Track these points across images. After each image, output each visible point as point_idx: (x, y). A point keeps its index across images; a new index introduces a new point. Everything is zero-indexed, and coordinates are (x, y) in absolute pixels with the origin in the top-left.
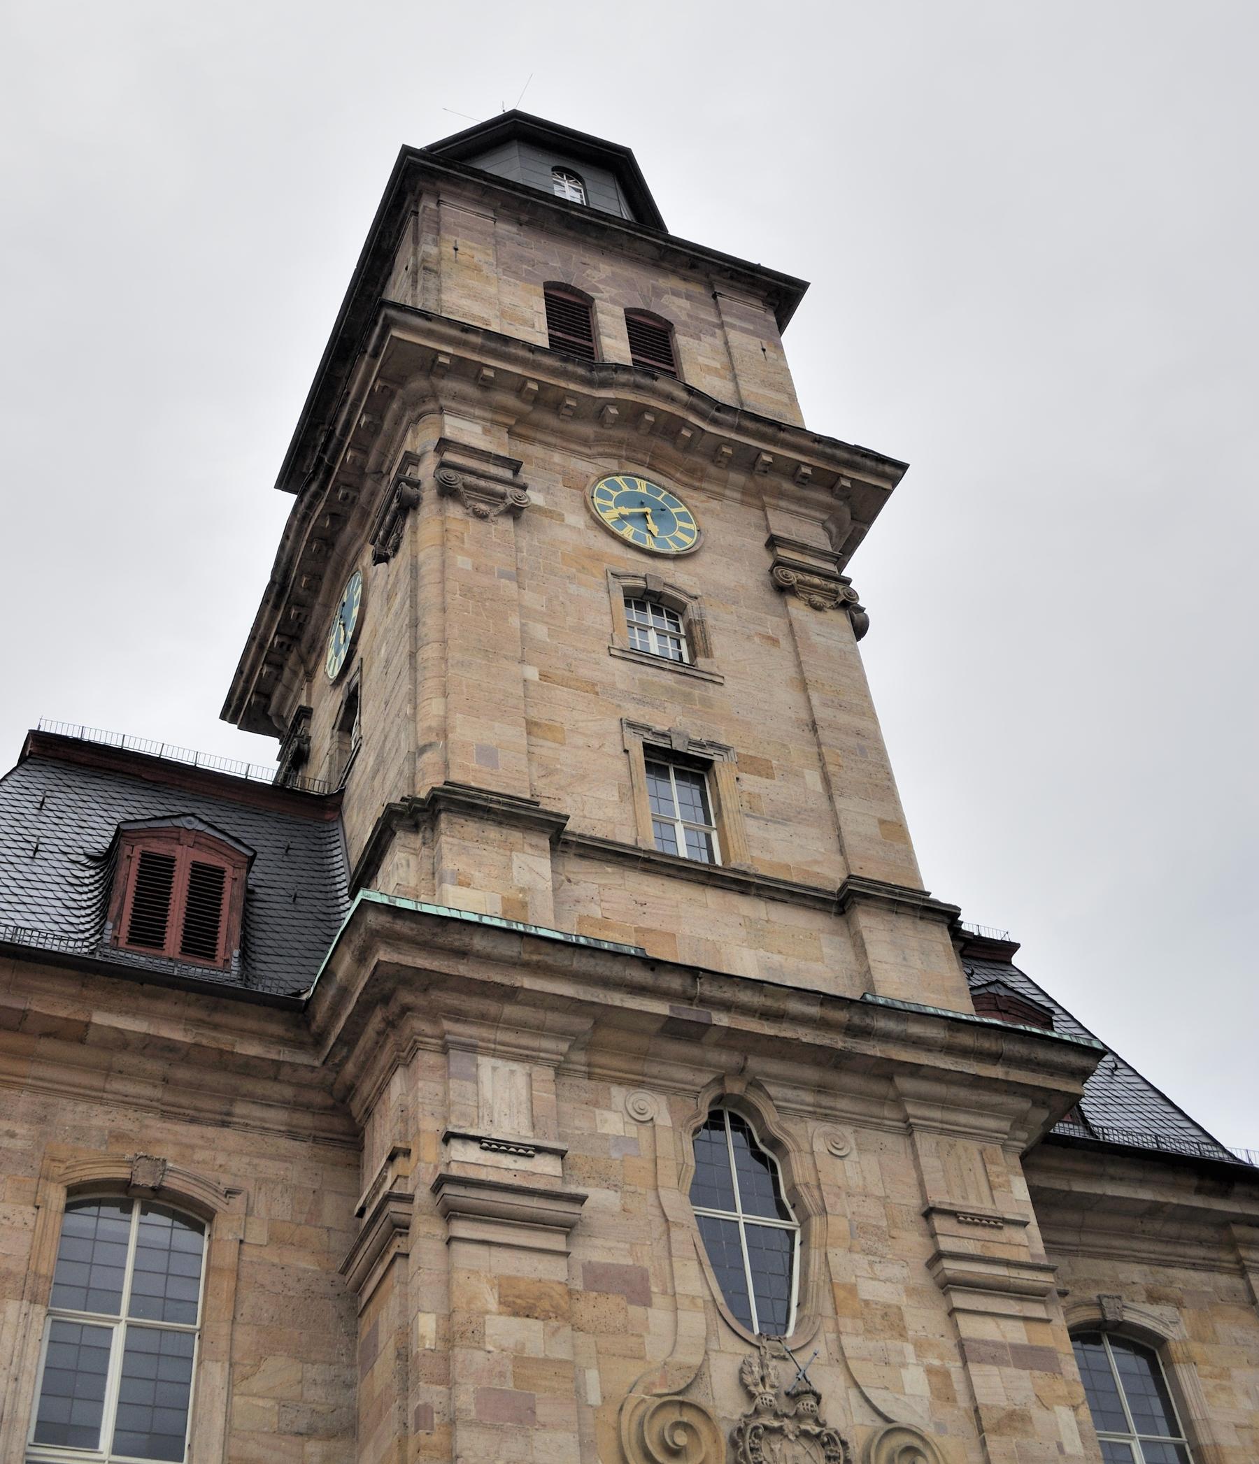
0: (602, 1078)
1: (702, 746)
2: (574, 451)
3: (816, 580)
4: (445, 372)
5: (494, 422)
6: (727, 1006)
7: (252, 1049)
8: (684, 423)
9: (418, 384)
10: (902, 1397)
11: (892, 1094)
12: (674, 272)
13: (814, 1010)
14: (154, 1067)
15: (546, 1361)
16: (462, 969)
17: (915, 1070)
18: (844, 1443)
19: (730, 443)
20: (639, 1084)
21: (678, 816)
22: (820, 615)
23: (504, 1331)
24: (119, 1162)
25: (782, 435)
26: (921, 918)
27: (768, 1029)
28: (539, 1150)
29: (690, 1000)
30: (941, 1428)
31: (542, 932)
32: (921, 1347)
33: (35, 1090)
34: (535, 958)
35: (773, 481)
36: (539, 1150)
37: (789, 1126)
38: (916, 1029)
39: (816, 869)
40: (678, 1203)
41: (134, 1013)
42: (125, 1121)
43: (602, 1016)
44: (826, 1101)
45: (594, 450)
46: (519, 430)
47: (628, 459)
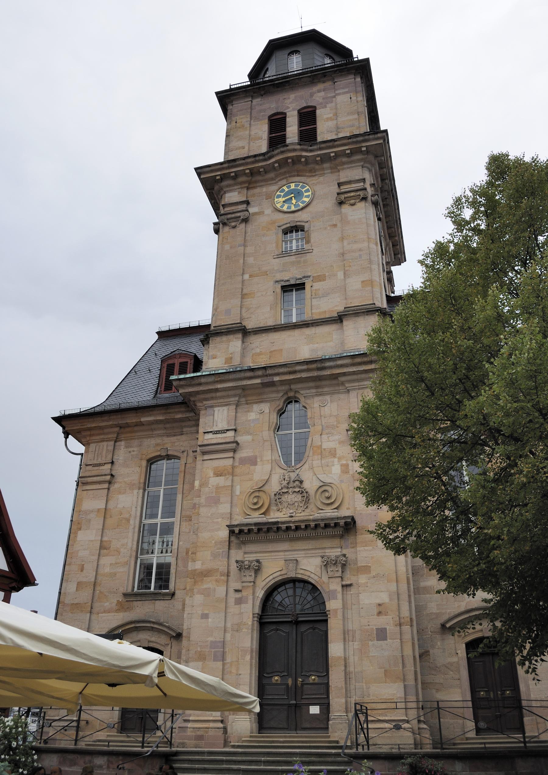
0: (250, 403)
1: (301, 279)
2: (270, 184)
3: (352, 194)
4: (222, 180)
5: (241, 188)
6: (278, 374)
7: (179, 416)
8: (301, 156)
9: (216, 187)
10: (330, 475)
11: (340, 383)
12: (319, 82)
13: (305, 367)
14: (160, 426)
15: (224, 487)
16: (201, 388)
17: (344, 374)
18: (307, 492)
19: (318, 156)
20: (262, 402)
21: (294, 306)
23: (214, 481)
24: (157, 451)
25: (336, 143)
26: (367, 315)
27: (292, 377)
28: (228, 430)
29: (267, 376)
30: (342, 481)
31: (220, 372)
32: (340, 459)
33: (138, 439)
34: (219, 379)
35: (339, 160)
36: (228, 430)
37: (308, 401)
38: (340, 362)
39: (336, 308)
40: (267, 434)
41: (150, 415)
42: (158, 440)
43: (244, 388)
44: (320, 390)
45: (277, 180)
46: (251, 186)
47: (290, 177)
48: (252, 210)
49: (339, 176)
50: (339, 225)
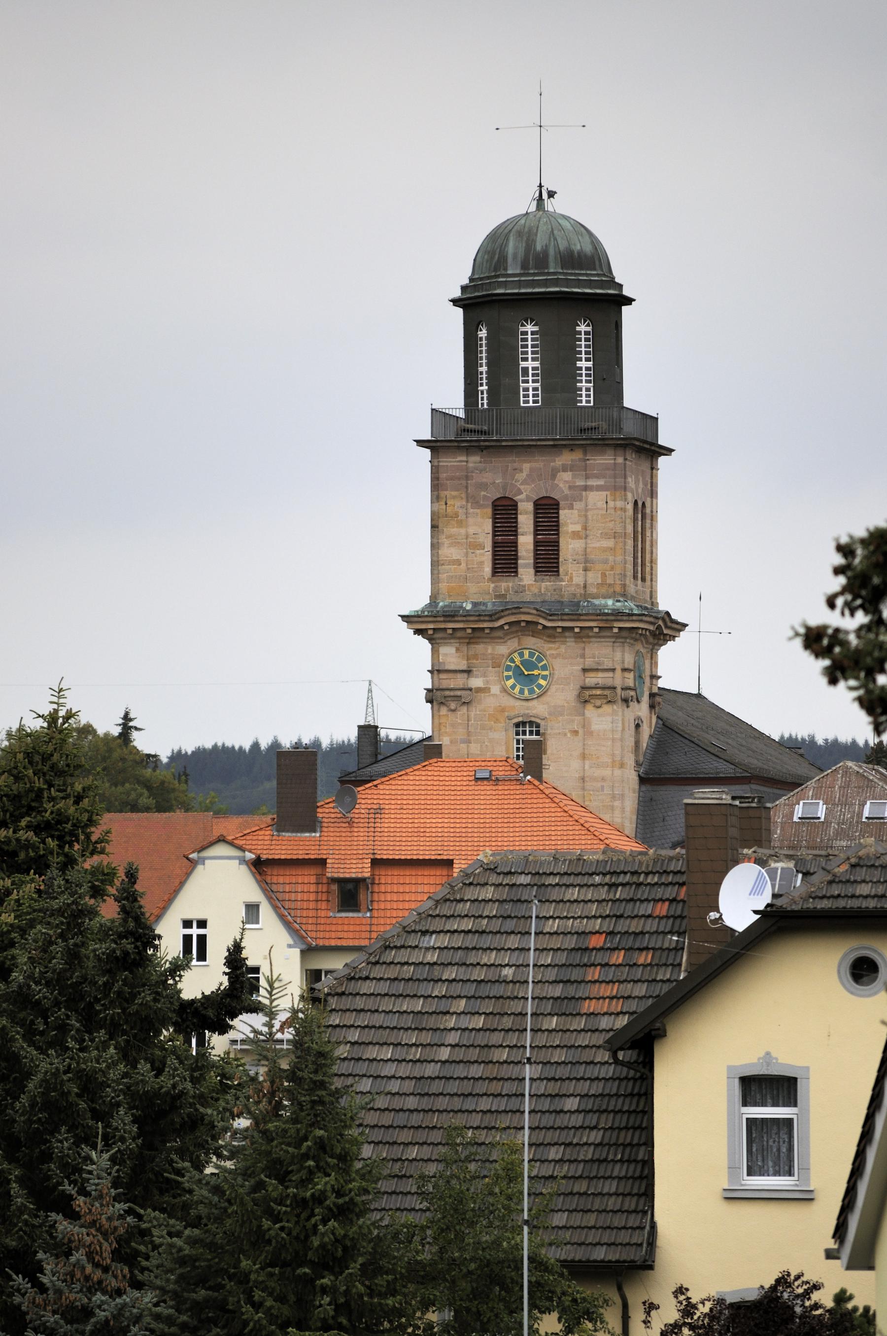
22: (600, 710)
25: (582, 618)
46: (472, 641)
48: (476, 682)
49: (584, 649)
50: (581, 732)
